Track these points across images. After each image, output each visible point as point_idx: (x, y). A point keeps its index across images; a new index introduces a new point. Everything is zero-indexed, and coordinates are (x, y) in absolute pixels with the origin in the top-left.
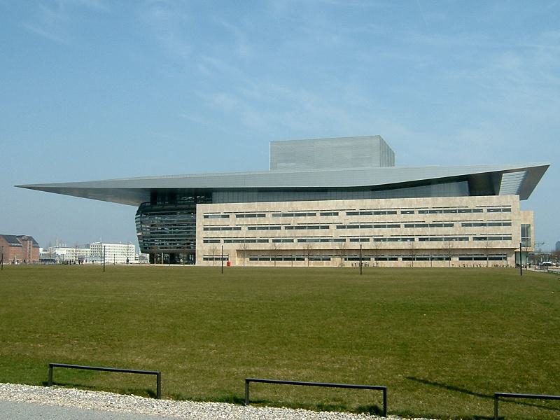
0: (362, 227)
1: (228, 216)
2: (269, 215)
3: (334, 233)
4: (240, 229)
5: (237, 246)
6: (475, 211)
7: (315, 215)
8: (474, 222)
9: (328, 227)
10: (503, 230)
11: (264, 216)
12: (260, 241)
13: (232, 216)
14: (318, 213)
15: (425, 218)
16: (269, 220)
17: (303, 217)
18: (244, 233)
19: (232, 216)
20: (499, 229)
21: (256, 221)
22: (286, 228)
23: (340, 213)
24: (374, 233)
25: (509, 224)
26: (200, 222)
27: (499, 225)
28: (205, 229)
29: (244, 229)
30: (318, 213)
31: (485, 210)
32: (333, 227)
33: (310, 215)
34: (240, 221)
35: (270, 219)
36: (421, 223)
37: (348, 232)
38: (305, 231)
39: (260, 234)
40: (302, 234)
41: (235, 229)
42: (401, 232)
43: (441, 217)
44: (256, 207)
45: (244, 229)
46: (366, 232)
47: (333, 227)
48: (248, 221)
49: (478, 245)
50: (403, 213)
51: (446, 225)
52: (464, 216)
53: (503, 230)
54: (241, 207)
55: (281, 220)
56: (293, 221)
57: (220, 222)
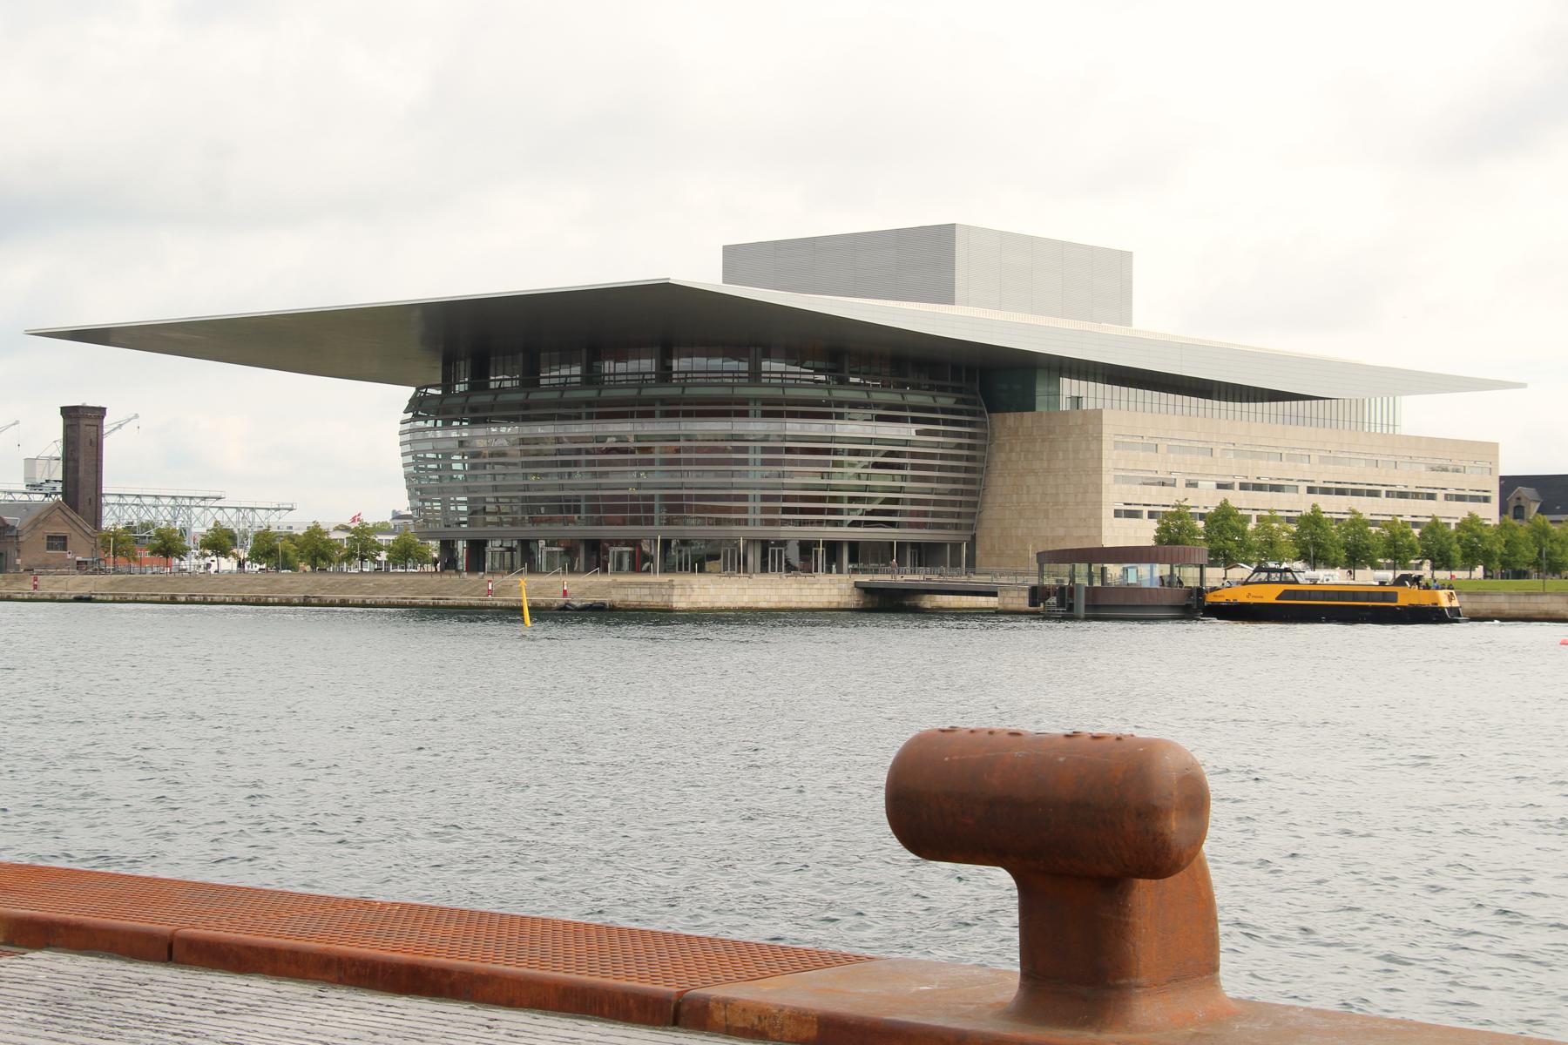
25: (1486, 500)
38: (1267, 495)
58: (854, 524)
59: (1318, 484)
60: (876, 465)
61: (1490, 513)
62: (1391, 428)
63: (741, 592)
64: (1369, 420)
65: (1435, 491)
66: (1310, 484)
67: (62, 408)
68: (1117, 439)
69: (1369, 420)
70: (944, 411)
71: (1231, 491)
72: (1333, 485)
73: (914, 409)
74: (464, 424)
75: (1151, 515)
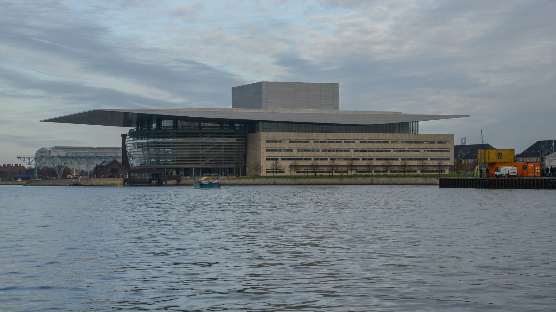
0: (369, 151)
3: (353, 155)
4: (292, 151)
5: (290, 162)
6: (431, 142)
7: (340, 142)
8: (431, 149)
9: (348, 151)
10: (445, 154)
11: (308, 142)
12: (305, 159)
14: (343, 141)
15: (405, 147)
16: (311, 145)
17: (334, 144)
18: (295, 154)
20: (444, 154)
22: (323, 151)
24: (376, 155)
25: (448, 151)
26: (264, 145)
27: (443, 151)
28: (267, 151)
29: (295, 150)
30: (343, 141)
31: (436, 142)
32: (352, 150)
33: (337, 142)
35: (313, 145)
36: (403, 149)
37: (361, 154)
38: (335, 153)
39: (306, 154)
40: (333, 155)
41: (288, 151)
42: (392, 154)
43: (413, 146)
44: (303, 136)
45: (295, 150)
46: (372, 154)
47: (352, 150)
48: (297, 145)
49: (432, 163)
51: (416, 151)
52: (425, 145)
53: (445, 154)
54: (293, 136)
56: (327, 146)
57: (278, 145)
58: (206, 163)
59: (360, 148)
60: (213, 149)
61: (451, 155)
62: (417, 131)
63: (108, 181)
64: (412, 129)
65: (419, 149)
66: (355, 149)
67: (122, 135)
68: (267, 140)
69: (412, 129)
70: (228, 134)
71: (318, 152)
72: (367, 149)
73: (224, 134)
74: (145, 138)
75: (282, 159)
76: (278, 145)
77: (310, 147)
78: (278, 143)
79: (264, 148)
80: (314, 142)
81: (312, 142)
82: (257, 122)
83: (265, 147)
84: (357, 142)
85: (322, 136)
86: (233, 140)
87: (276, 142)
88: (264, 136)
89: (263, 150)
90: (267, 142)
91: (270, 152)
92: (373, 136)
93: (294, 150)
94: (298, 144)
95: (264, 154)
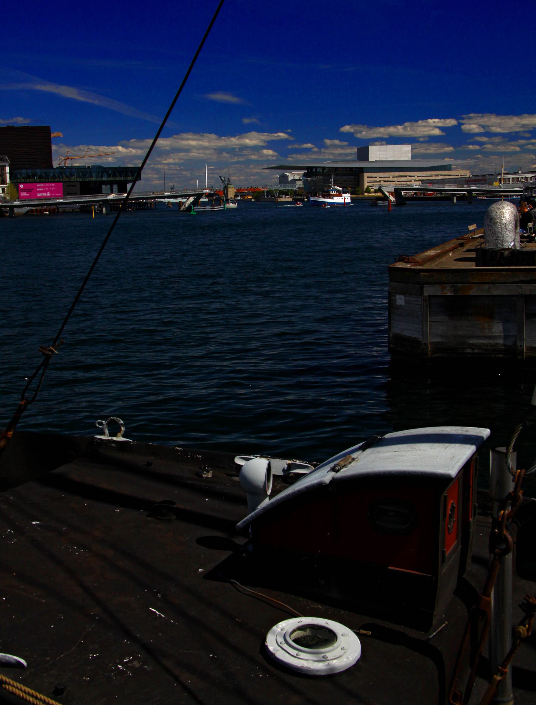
1: (376, 178)
2: (391, 177)
7: (407, 177)
9: (411, 181)
11: (389, 177)
13: (378, 177)
14: (408, 176)
16: (391, 179)
19: (378, 177)
21: (386, 179)
23: (415, 176)
26: (366, 180)
28: (368, 182)
30: (408, 176)
32: (413, 181)
34: (381, 179)
44: (387, 174)
45: (382, 182)
47: (413, 181)
50: (435, 176)
54: (381, 174)
55: (395, 179)
56: (400, 179)
57: (373, 179)
76: (373, 179)
77: (390, 180)
78: (373, 179)
79: (366, 181)
80: (393, 177)
81: (391, 177)
82: (364, 168)
83: (366, 180)
84: (416, 176)
85: (397, 174)
86: (352, 177)
87: (372, 178)
88: (366, 175)
89: (366, 182)
90: (368, 178)
91: (369, 183)
92: (425, 173)
93: (382, 182)
94: (384, 178)
95: (366, 185)
